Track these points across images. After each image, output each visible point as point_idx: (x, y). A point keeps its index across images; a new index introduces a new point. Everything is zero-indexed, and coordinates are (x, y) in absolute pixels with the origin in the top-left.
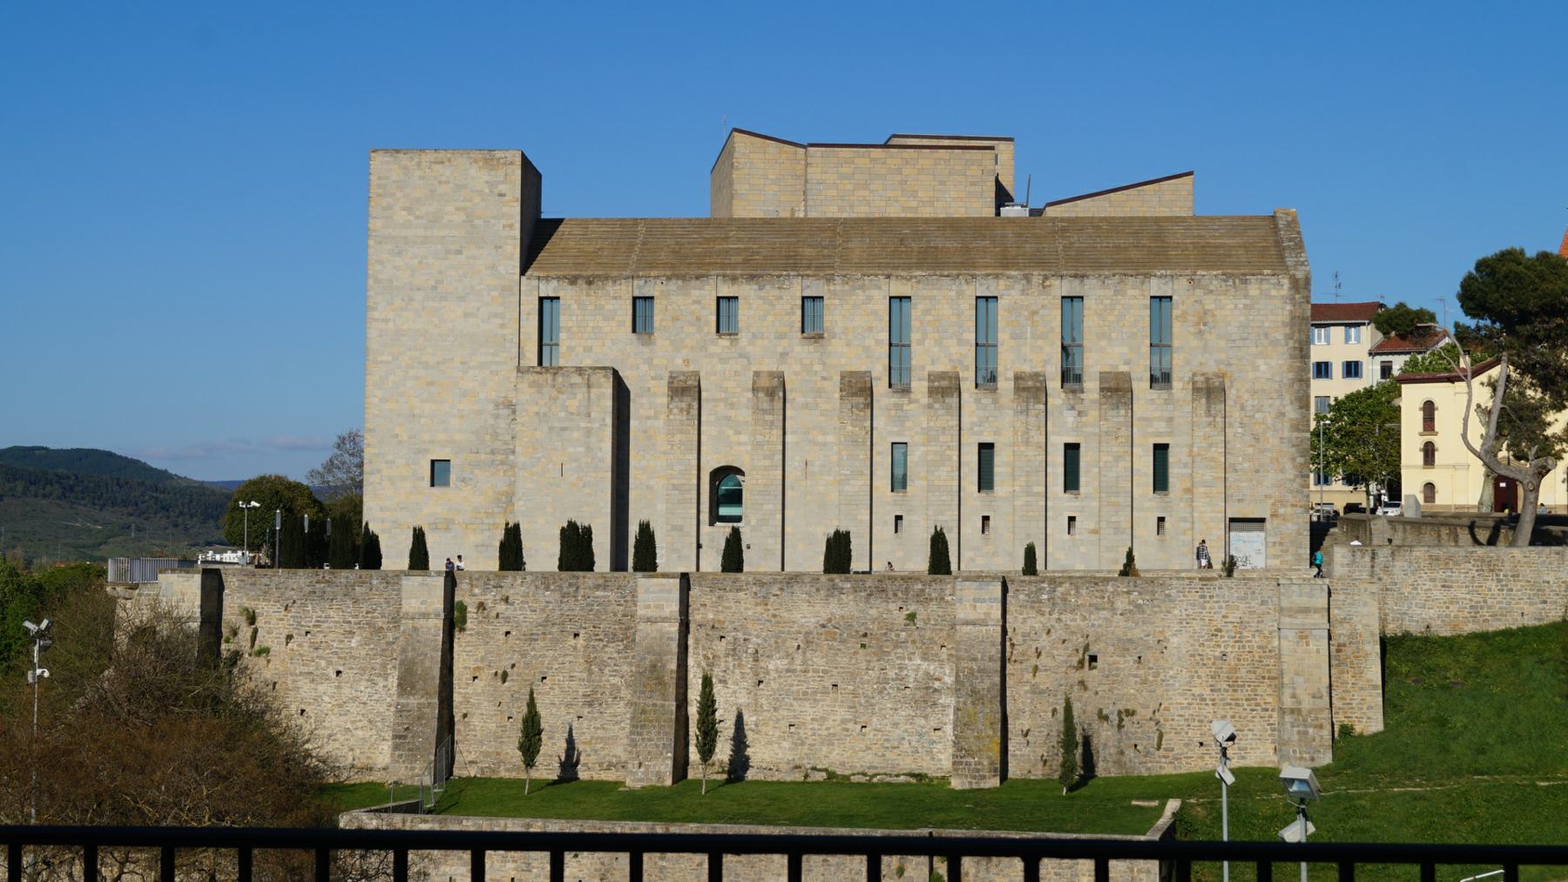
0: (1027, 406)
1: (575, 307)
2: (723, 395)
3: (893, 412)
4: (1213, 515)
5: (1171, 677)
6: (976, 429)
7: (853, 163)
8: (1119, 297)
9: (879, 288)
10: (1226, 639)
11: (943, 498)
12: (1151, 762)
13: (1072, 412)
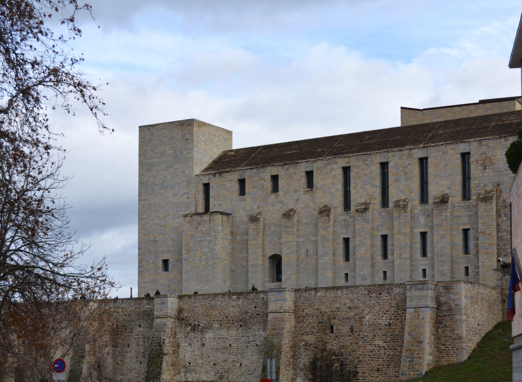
0: (400, 214)
1: (215, 187)
2: (273, 221)
3: (343, 223)
4: (489, 264)
5: (365, 336)
6: (380, 228)
7: (445, 115)
8: (445, 155)
9: (336, 163)
10: (390, 315)
11: (363, 263)
12: (355, 379)
13: (423, 216)
